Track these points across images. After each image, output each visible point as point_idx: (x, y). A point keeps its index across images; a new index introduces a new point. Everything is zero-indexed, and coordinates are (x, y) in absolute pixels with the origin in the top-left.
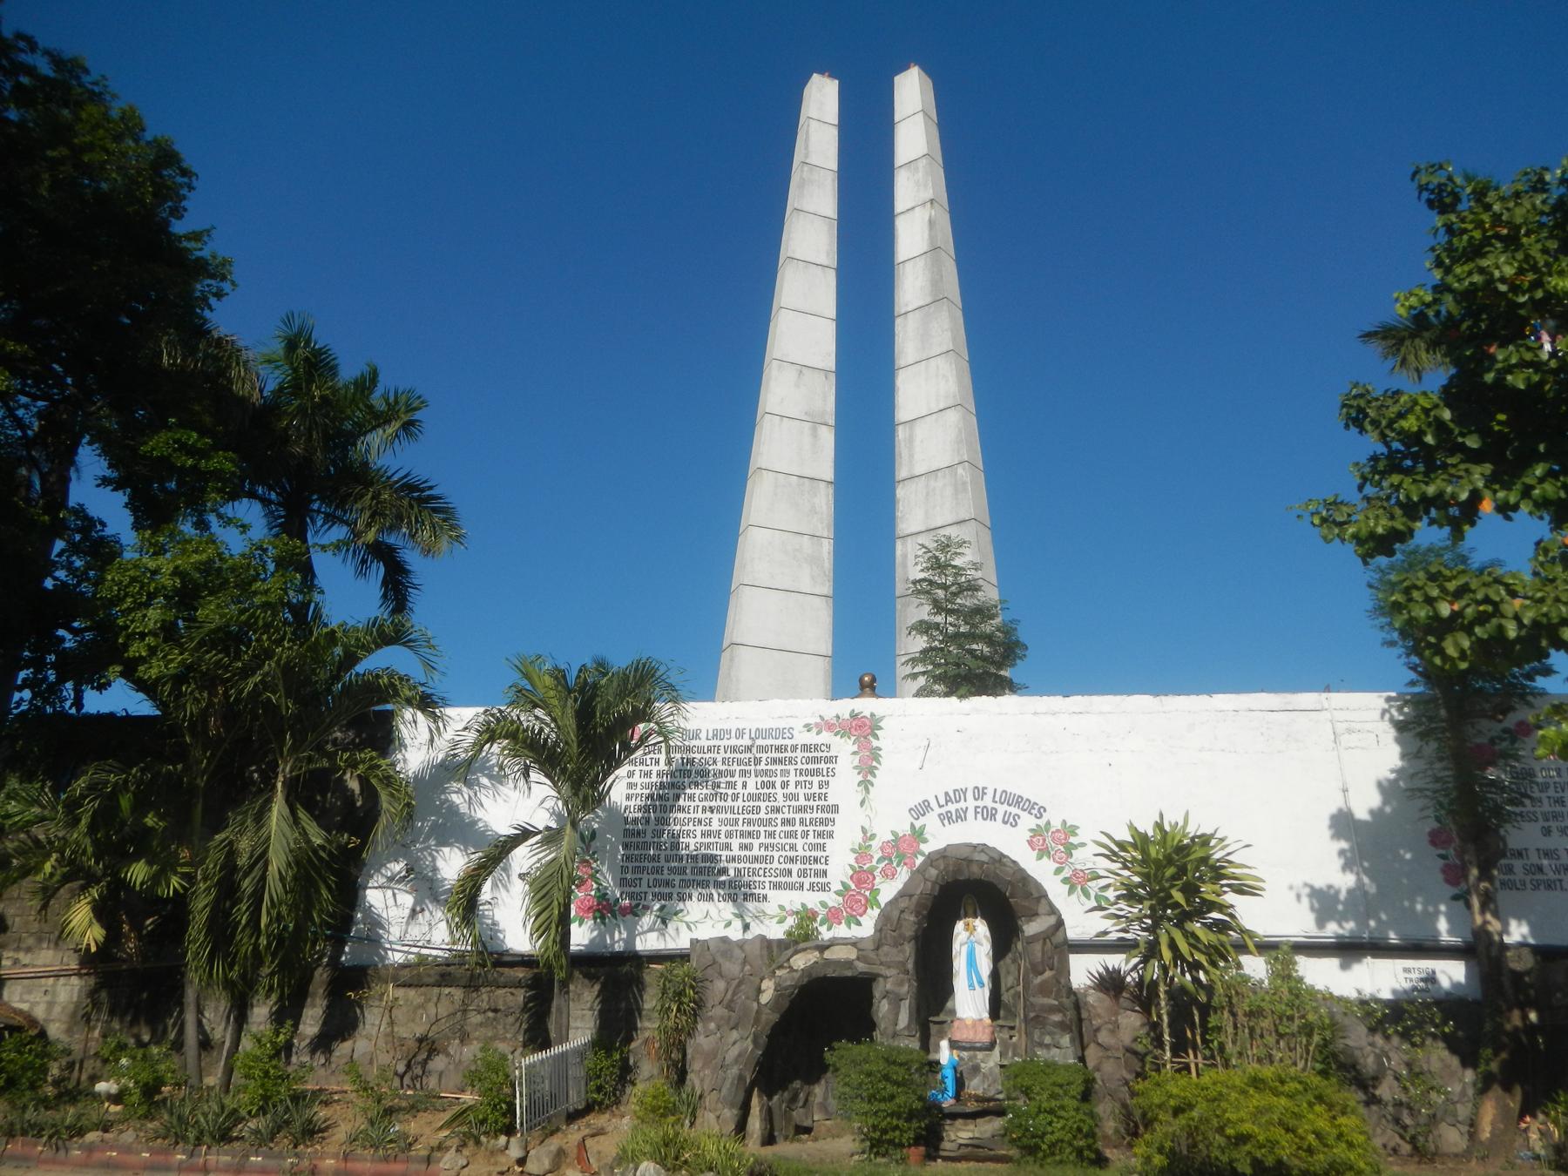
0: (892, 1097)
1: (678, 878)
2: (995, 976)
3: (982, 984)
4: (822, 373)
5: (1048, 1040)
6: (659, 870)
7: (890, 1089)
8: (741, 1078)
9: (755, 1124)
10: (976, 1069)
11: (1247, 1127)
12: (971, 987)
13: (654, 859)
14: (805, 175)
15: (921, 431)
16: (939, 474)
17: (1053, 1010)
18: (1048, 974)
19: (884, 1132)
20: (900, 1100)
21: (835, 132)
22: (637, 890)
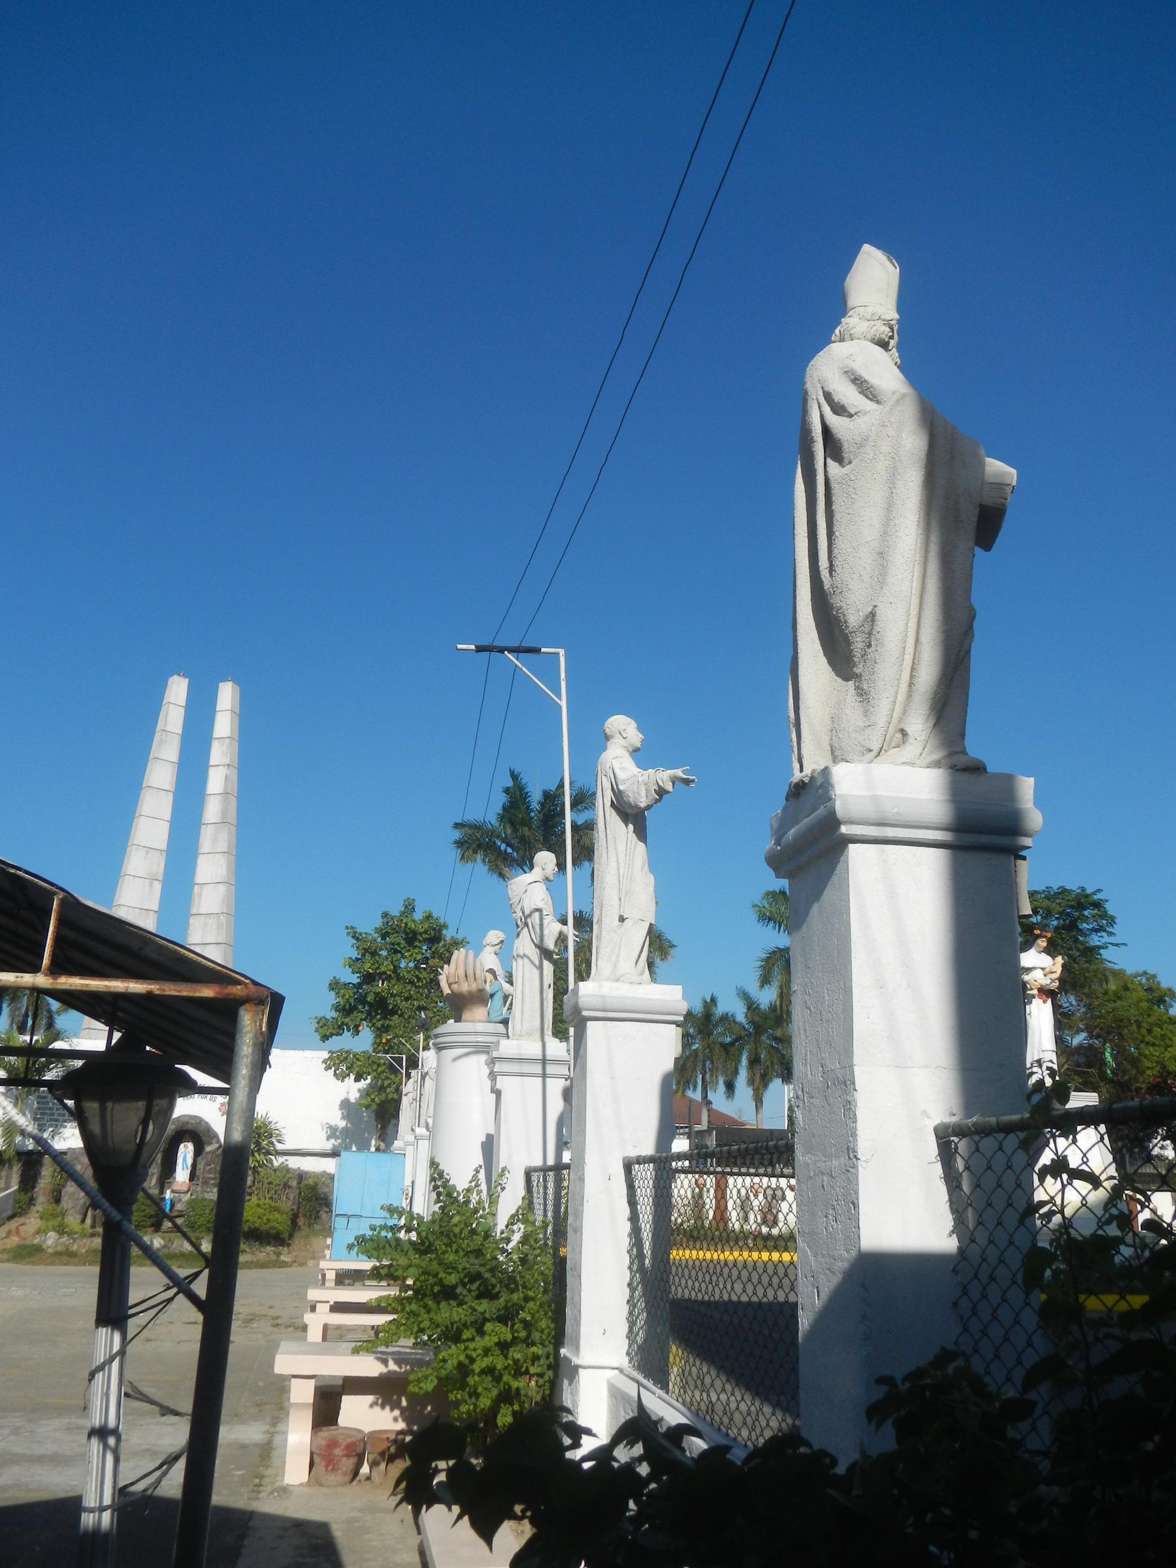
0: (144, 1210)
1: (61, 1118)
2: (194, 1166)
3: (187, 1168)
4: (159, 852)
5: (208, 1190)
6: (52, 1114)
7: (144, 1207)
8: (85, 1203)
9: (89, 1221)
10: (180, 1200)
11: (249, 1218)
12: (183, 1169)
13: (51, 1109)
14: (163, 737)
15: (206, 891)
16: (212, 916)
17: (212, 1179)
18: (212, 1166)
19: (140, 1222)
20: (147, 1211)
21: (182, 710)
22: (42, 1122)
